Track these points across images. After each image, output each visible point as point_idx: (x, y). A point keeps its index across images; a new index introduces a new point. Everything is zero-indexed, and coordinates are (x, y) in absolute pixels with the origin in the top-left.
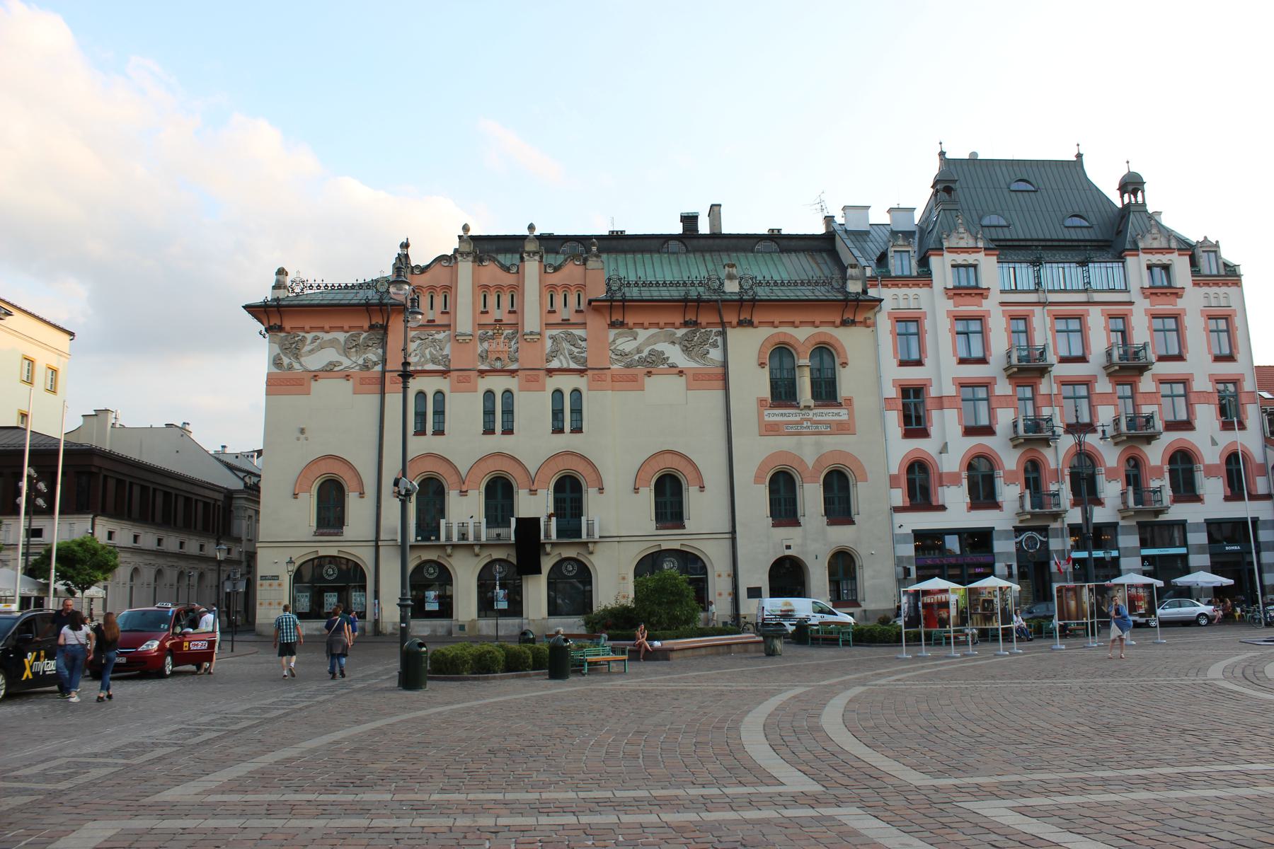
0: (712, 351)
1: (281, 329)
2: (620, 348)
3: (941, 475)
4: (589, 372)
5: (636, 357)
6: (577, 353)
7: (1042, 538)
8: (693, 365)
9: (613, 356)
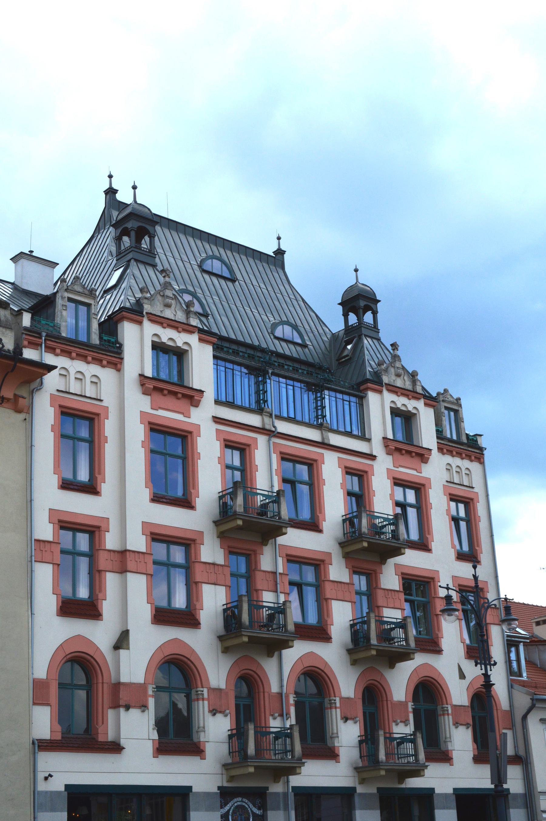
3: (117, 686)
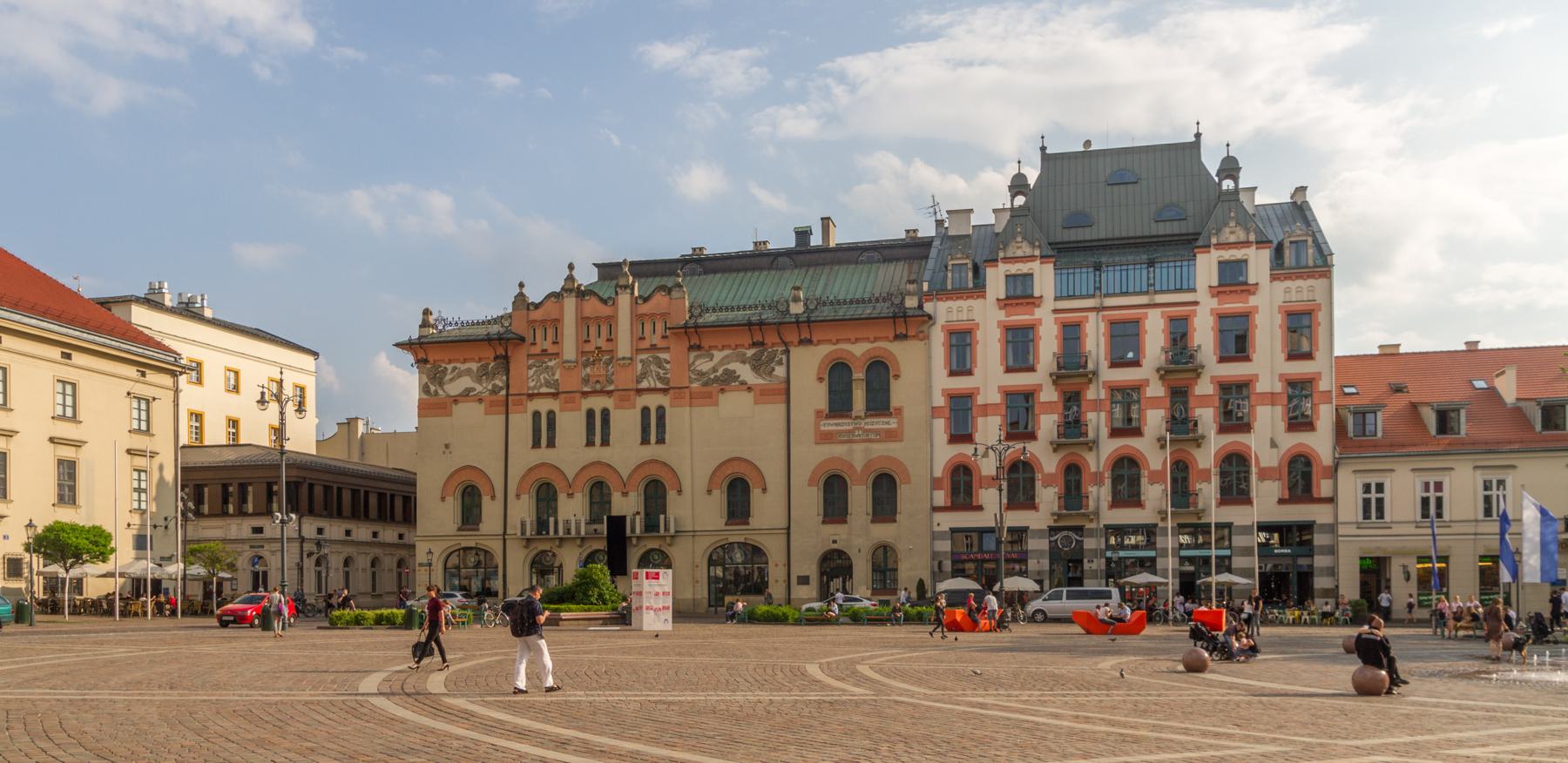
0: (777, 368)
1: (426, 361)
2: (698, 368)
4: (672, 391)
5: (712, 376)
6: (663, 374)
7: (1078, 538)
8: (760, 381)
9: (693, 376)
